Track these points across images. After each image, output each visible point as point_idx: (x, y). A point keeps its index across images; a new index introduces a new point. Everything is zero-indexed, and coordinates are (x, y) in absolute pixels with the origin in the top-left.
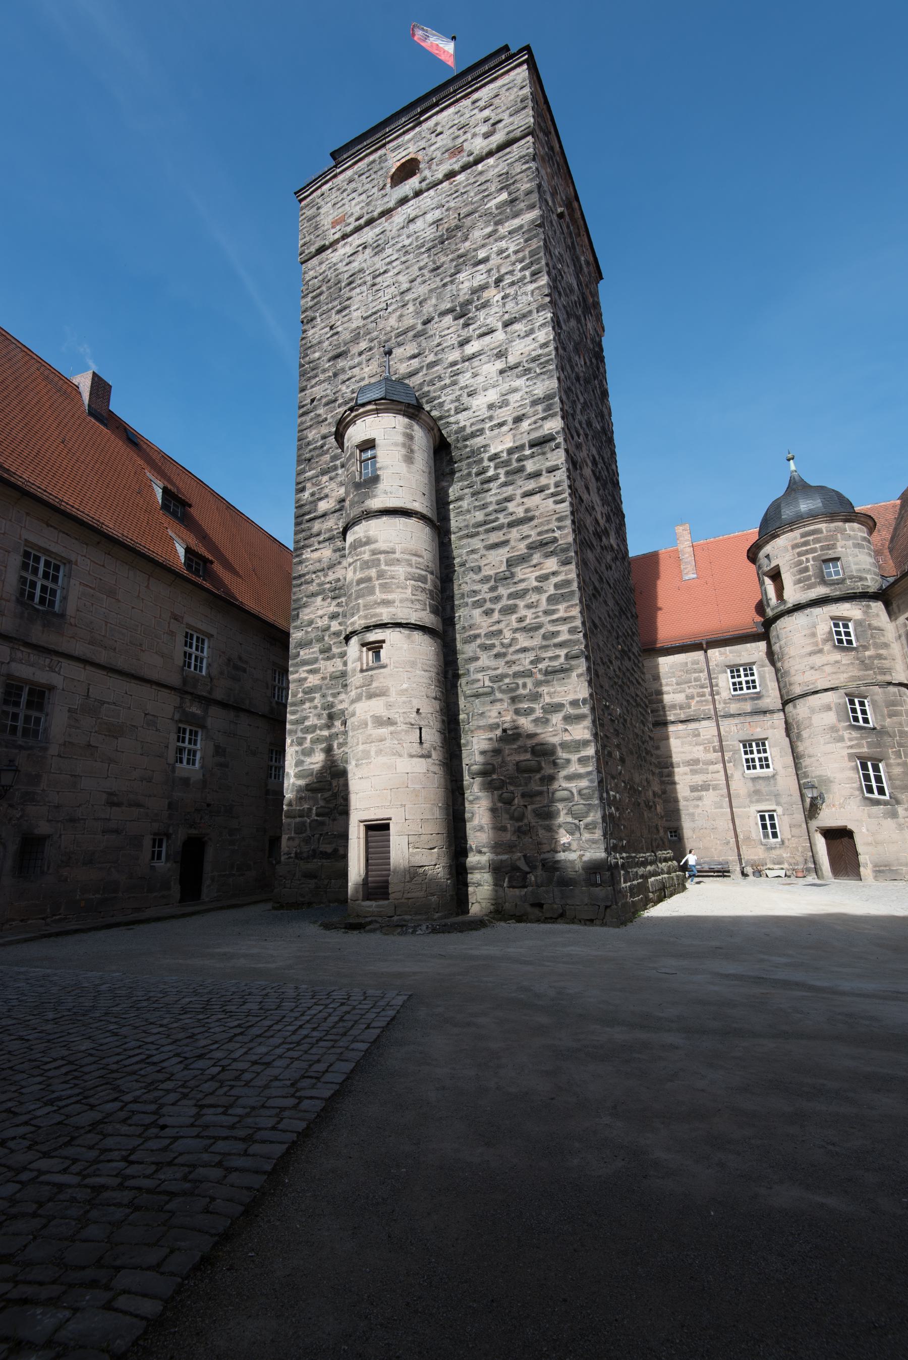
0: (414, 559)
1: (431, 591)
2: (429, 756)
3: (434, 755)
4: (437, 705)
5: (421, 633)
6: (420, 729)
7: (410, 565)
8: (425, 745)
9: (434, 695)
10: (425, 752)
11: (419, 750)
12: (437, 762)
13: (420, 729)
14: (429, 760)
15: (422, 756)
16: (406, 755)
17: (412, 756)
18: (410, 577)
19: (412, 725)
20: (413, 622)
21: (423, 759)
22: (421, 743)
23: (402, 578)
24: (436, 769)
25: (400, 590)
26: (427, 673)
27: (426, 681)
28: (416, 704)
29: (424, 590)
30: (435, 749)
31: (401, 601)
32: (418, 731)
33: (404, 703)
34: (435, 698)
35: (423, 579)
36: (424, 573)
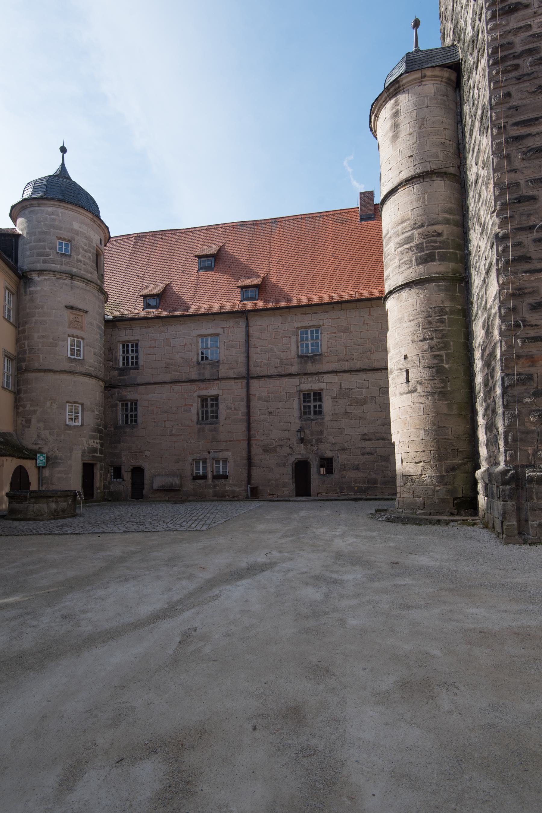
0: (400, 228)
1: (417, 246)
2: (414, 391)
3: (420, 389)
4: (425, 345)
5: (407, 290)
6: (407, 371)
7: (398, 235)
8: (411, 383)
9: (422, 337)
10: (411, 388)
11: (406, 388)
12: (423, 394)
13: (407, 371)
14: (415, 394)
15: (410, 392)
16: (398, 395)
17: (401, 394)
18: (398, 246)
19: (401, 369)
20: (400, 284)
21: (409, 395)
22: (408, 381)
23: (393, 251)
24: (422, 400)
25: (392, 262)
26: (412, 322)
27: (411, 329)
28: (404, 352)
29: (410, 249)
30: (421, 383)
31: (393, 271)
32: (405, 373)
33: (397, 354)
34: (424, 339)
35: (411, 239)
36: (409, 234)
